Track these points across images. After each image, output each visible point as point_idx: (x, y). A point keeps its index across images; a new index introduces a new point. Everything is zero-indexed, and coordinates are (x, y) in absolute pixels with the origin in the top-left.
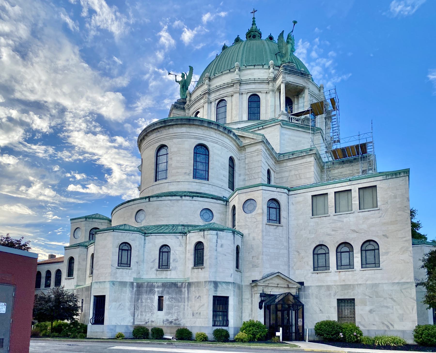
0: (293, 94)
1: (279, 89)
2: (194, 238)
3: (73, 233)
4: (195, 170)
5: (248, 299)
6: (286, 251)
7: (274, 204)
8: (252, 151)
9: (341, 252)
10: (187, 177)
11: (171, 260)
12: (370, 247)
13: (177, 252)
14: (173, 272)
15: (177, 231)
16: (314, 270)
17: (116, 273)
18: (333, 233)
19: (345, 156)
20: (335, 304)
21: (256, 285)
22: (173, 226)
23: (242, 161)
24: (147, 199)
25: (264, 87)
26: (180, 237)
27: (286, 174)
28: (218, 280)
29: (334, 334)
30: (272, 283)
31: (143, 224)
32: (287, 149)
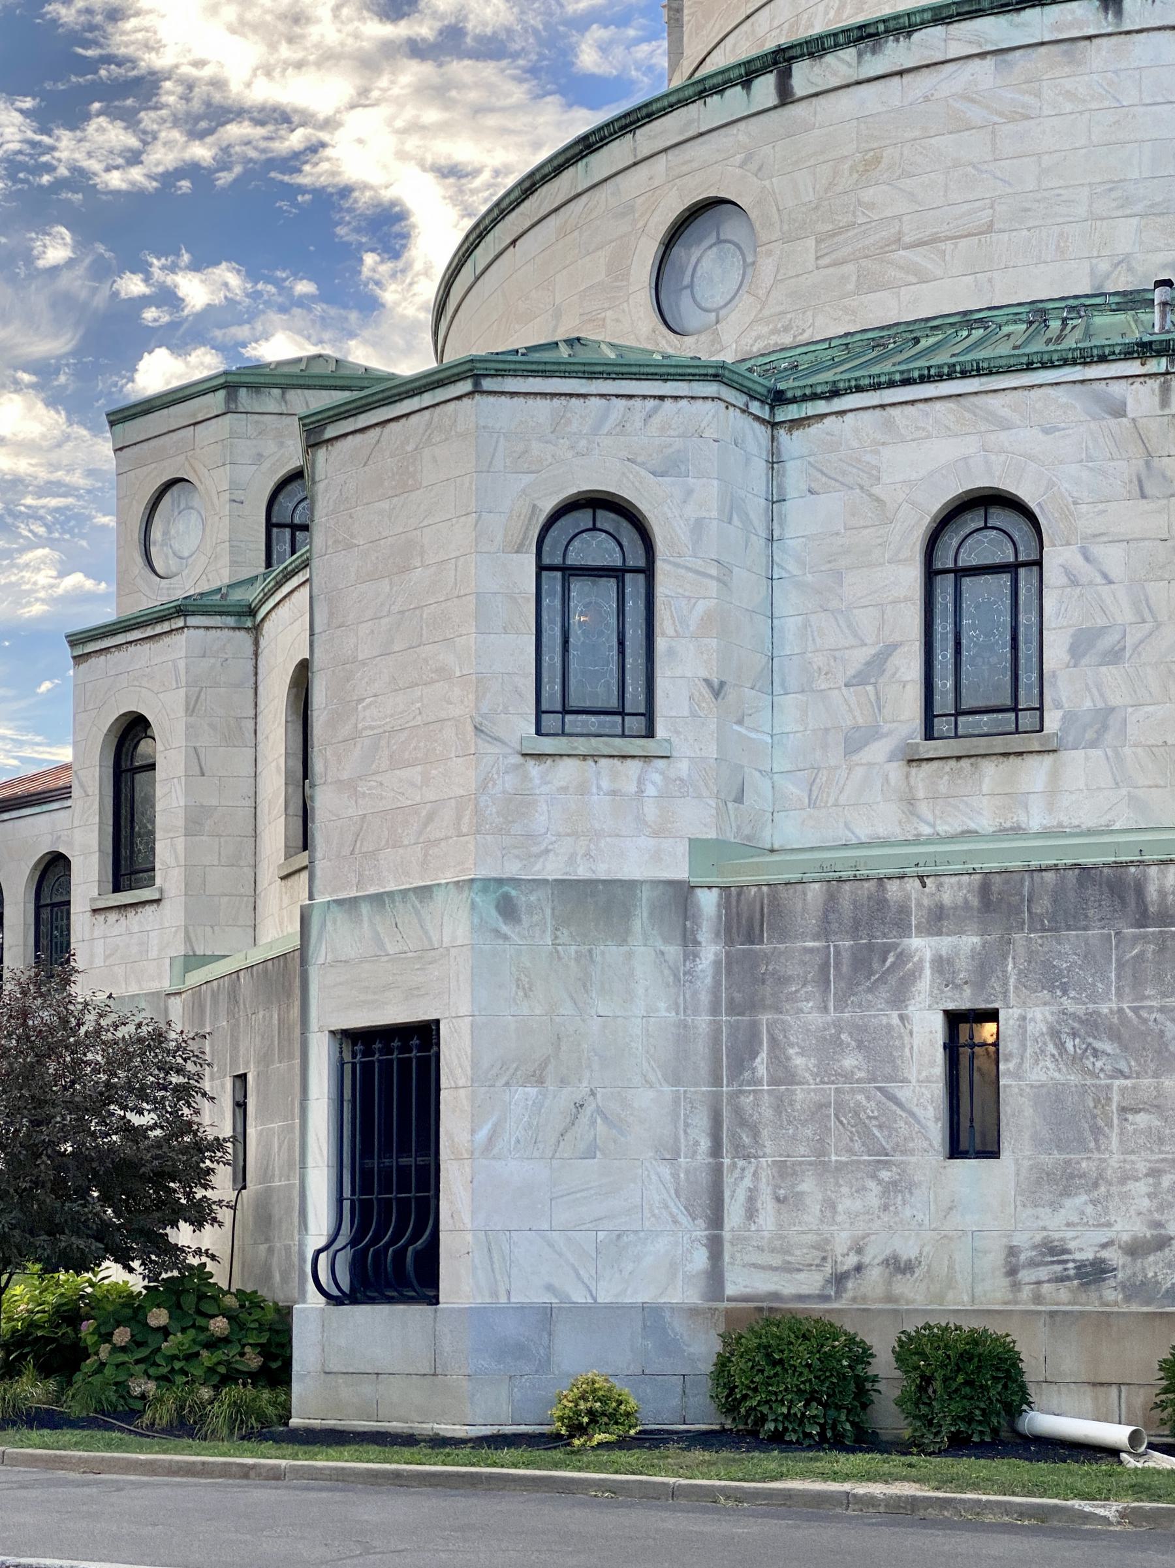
3: (136, 534)
13: (1113, 557)
14: (1078, 764)
24: (766, 86)
26: (1141, 398)
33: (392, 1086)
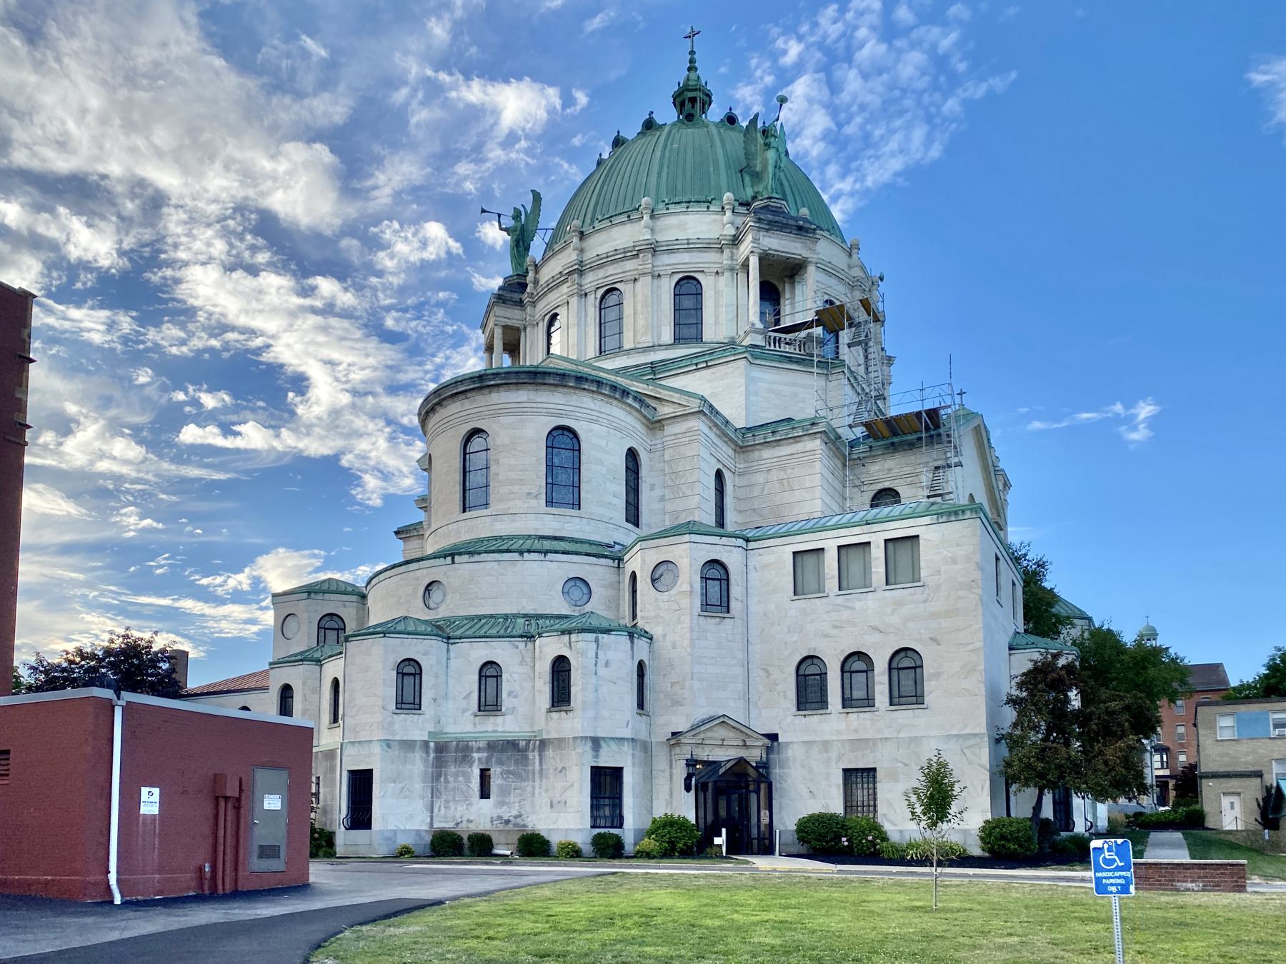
0: (776, 280)
1: (745, 266)
2: (550, 647)
4: (551, 485)
5: (663, 771)
6: (739, 670)
7: (716, 572)
8: (679, 431)
9: (851, 672)
10: (533, 503)
11: (504, 695)
12: (907, 663)
13: (516, 676)
15: (515, 633)
16: (799, 709)
17: (391, 724)
18: (834, 632)
19: (895, 434)
21: (678, 744)
22: (506, 617)
24: (449, 559)
25: (712, 256)
26: (521, 645)
27: (760, 478)
28: (601, 734)
29: (831, 840)
31: (442, 613)
33: (361, 783)
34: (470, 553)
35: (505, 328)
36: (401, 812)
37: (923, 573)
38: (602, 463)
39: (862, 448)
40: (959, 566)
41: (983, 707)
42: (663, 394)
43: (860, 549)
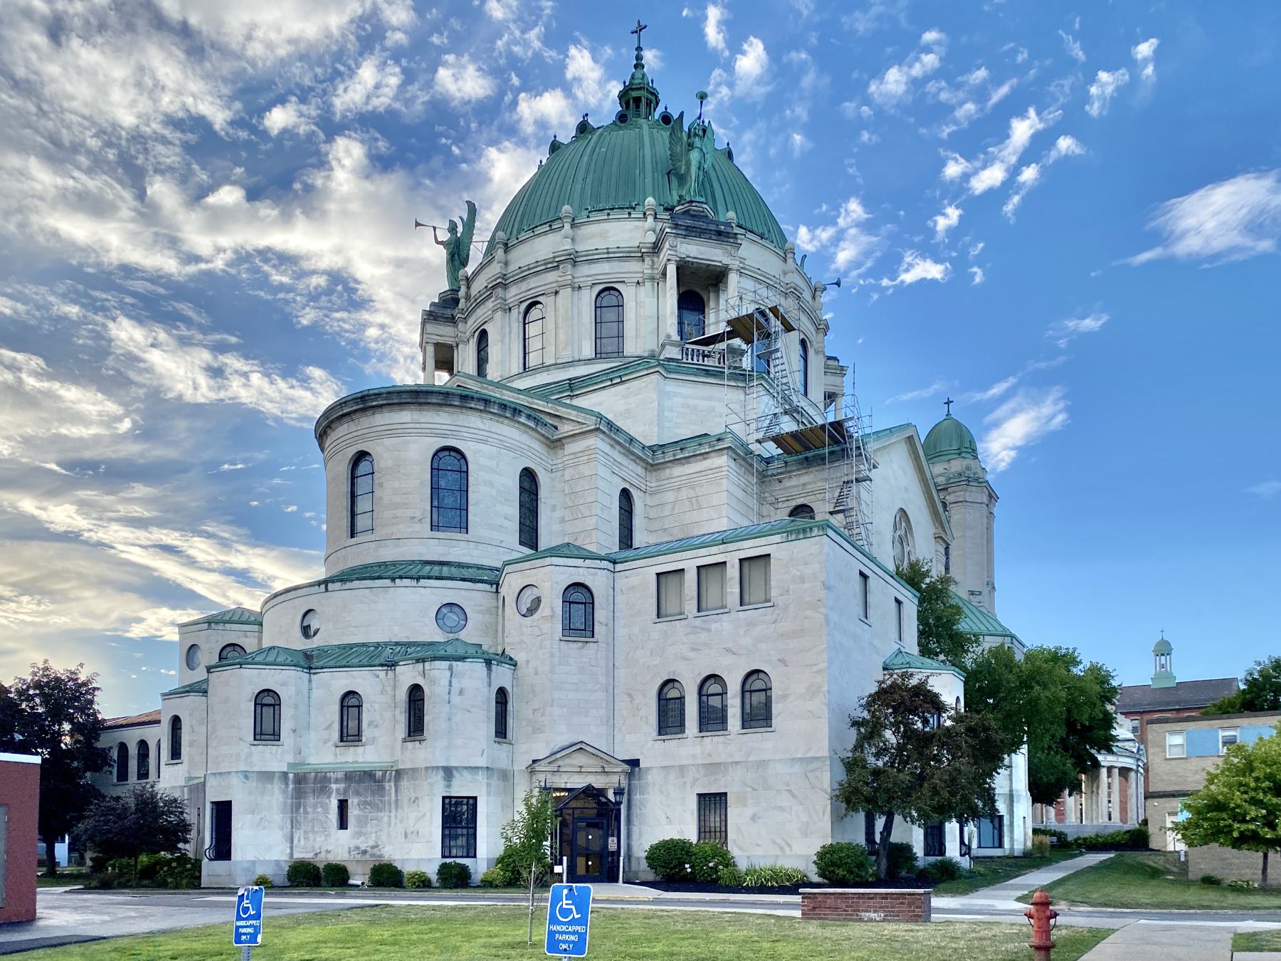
2: (408, 674)
10: (417, 527)
12: (758, 685)
13: (376, 706)
14: (368, 747)
16: (660, 734)
17: (249, 755)
18: (692, 654)
20: (693, 803)
22: (378, 645)
23: (559, 474)
24: (323, 586)
25: (634, 268)
27: (670, 496)
28: (453, 763)
29: (675, 867)
30: (565, 766)
32: (678, 431)
34: (341, 581)
35: (437, 345)
36: (261, 842)
37: (774, 593)
38: (491, 484)
39: (776, 464)
40: (806, 586)
41: (826, 730)
42: (562, 411)
43: (718, 569)
